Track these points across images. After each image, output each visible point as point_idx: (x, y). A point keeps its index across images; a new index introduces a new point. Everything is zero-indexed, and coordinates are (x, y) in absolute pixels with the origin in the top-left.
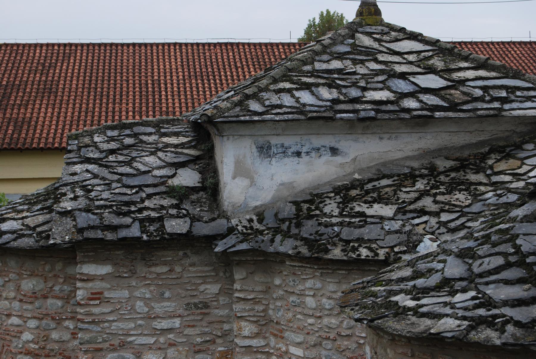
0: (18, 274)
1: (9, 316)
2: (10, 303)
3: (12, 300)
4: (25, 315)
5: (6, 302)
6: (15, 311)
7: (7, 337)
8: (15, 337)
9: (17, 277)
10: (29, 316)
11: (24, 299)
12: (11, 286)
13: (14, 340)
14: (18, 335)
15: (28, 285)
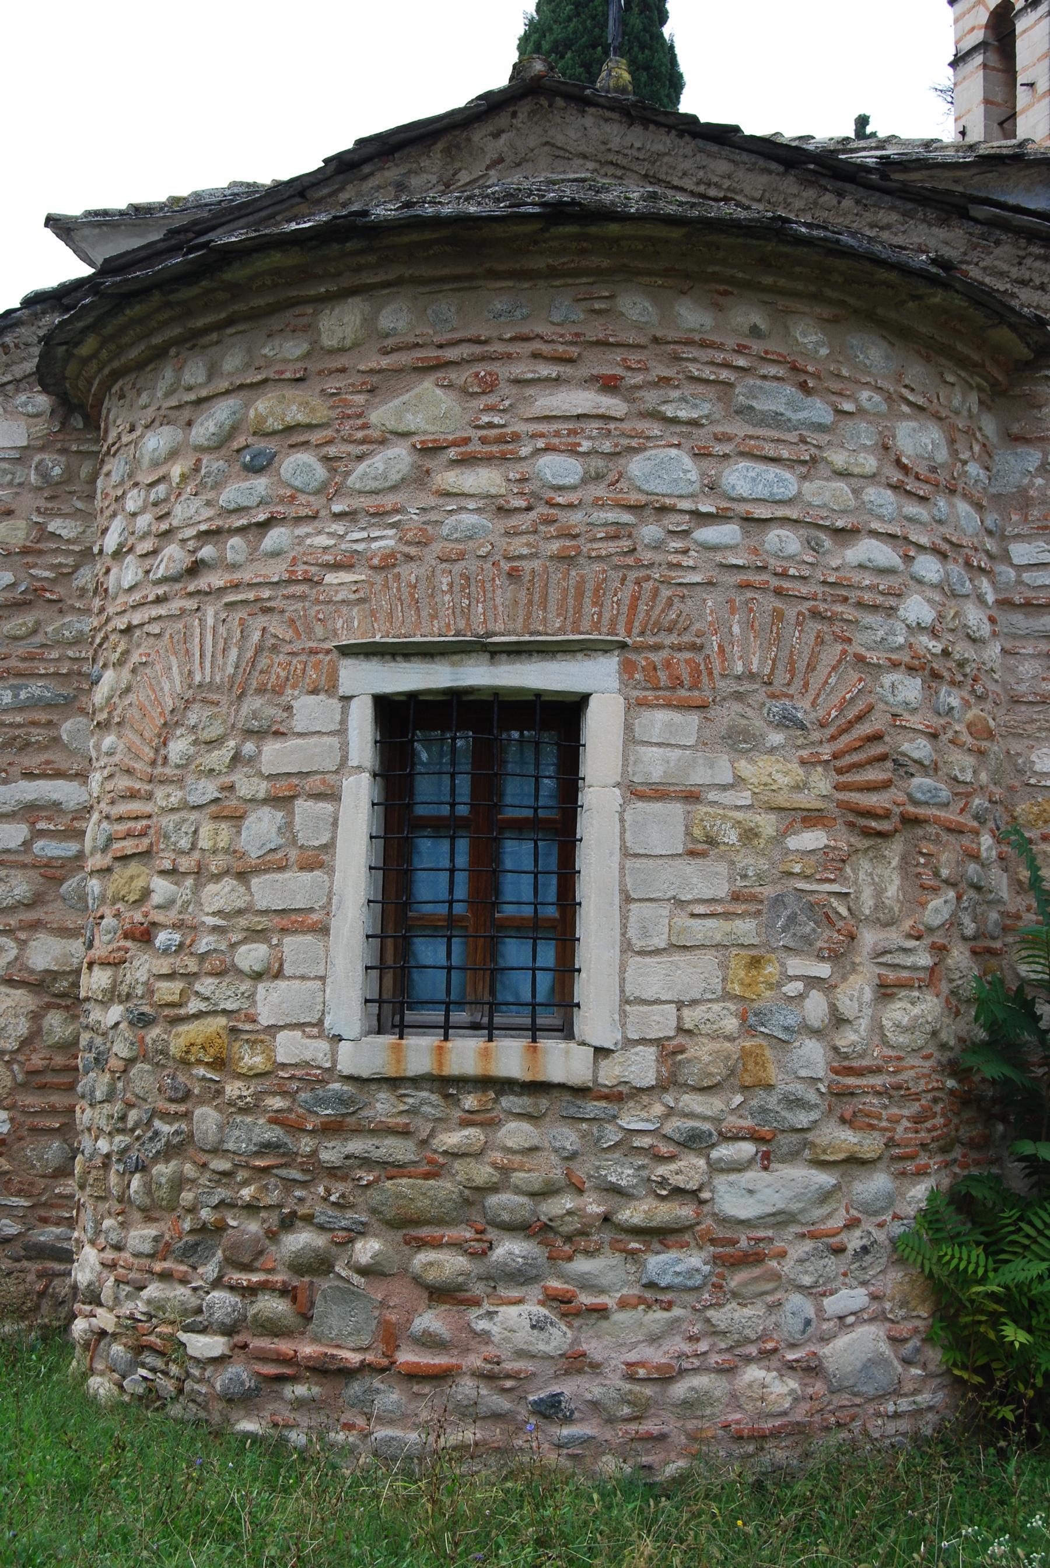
0: (889, 398)
1: (845, 535)
2: (856, 492)
3: (862, 482)
4: (913, 538)
5: (841, 485)
6: (880, 518)
7: (839, 608)
8: (875, 608)
9: (884, 407)
10: (924, 540)
11: (906, 479)
12: (865, 433)
13: (868, 619)
14: (892, 602)
15: (919, 440)
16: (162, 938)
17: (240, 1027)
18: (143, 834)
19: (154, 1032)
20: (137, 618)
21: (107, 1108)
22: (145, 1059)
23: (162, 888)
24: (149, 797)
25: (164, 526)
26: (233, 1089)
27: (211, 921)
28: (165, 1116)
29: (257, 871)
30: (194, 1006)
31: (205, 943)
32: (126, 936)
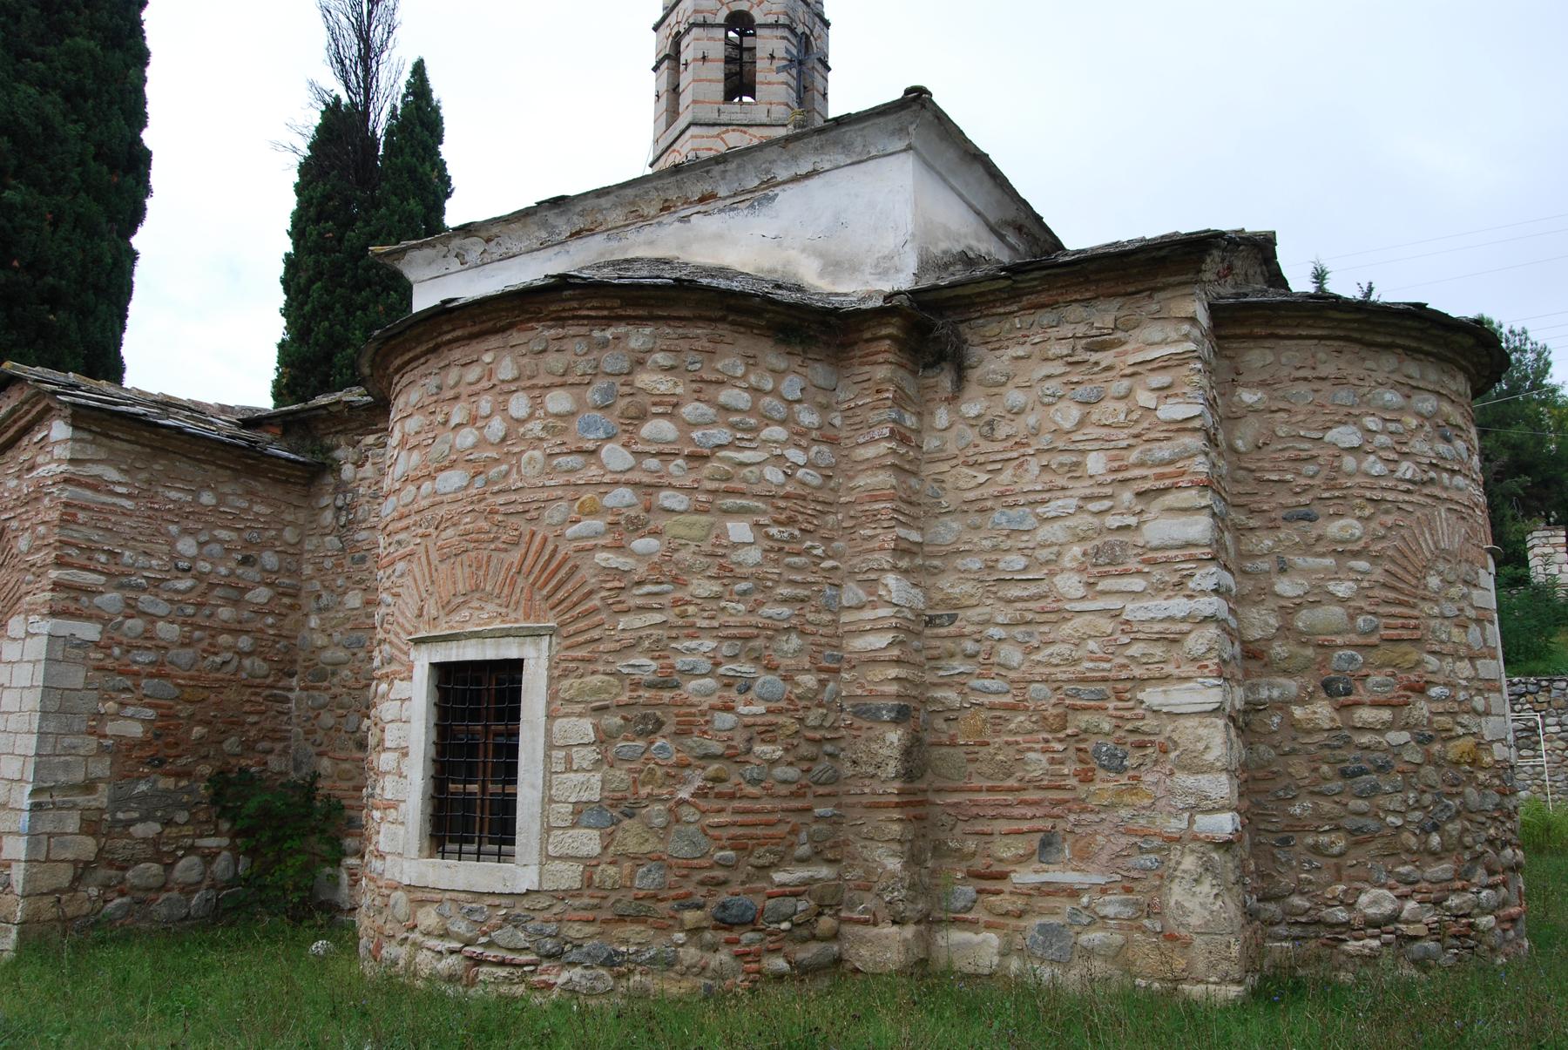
16: (1434, 691)
17: (1481, 745)
18: (1416, 628)
19: (1436, 747)
20: (1390, 496)
21: (1400, 796)
22: (1429, 763)
23: (1433, 662)
24: (1414, 607)
25: (1405, 449)
26: (1481, 776)
27: (1464, 683)
28: (1450, 796)
29: (1479, 657)
30: (1460, 731)
31: (1462, 695)
32: (1406, 688)
